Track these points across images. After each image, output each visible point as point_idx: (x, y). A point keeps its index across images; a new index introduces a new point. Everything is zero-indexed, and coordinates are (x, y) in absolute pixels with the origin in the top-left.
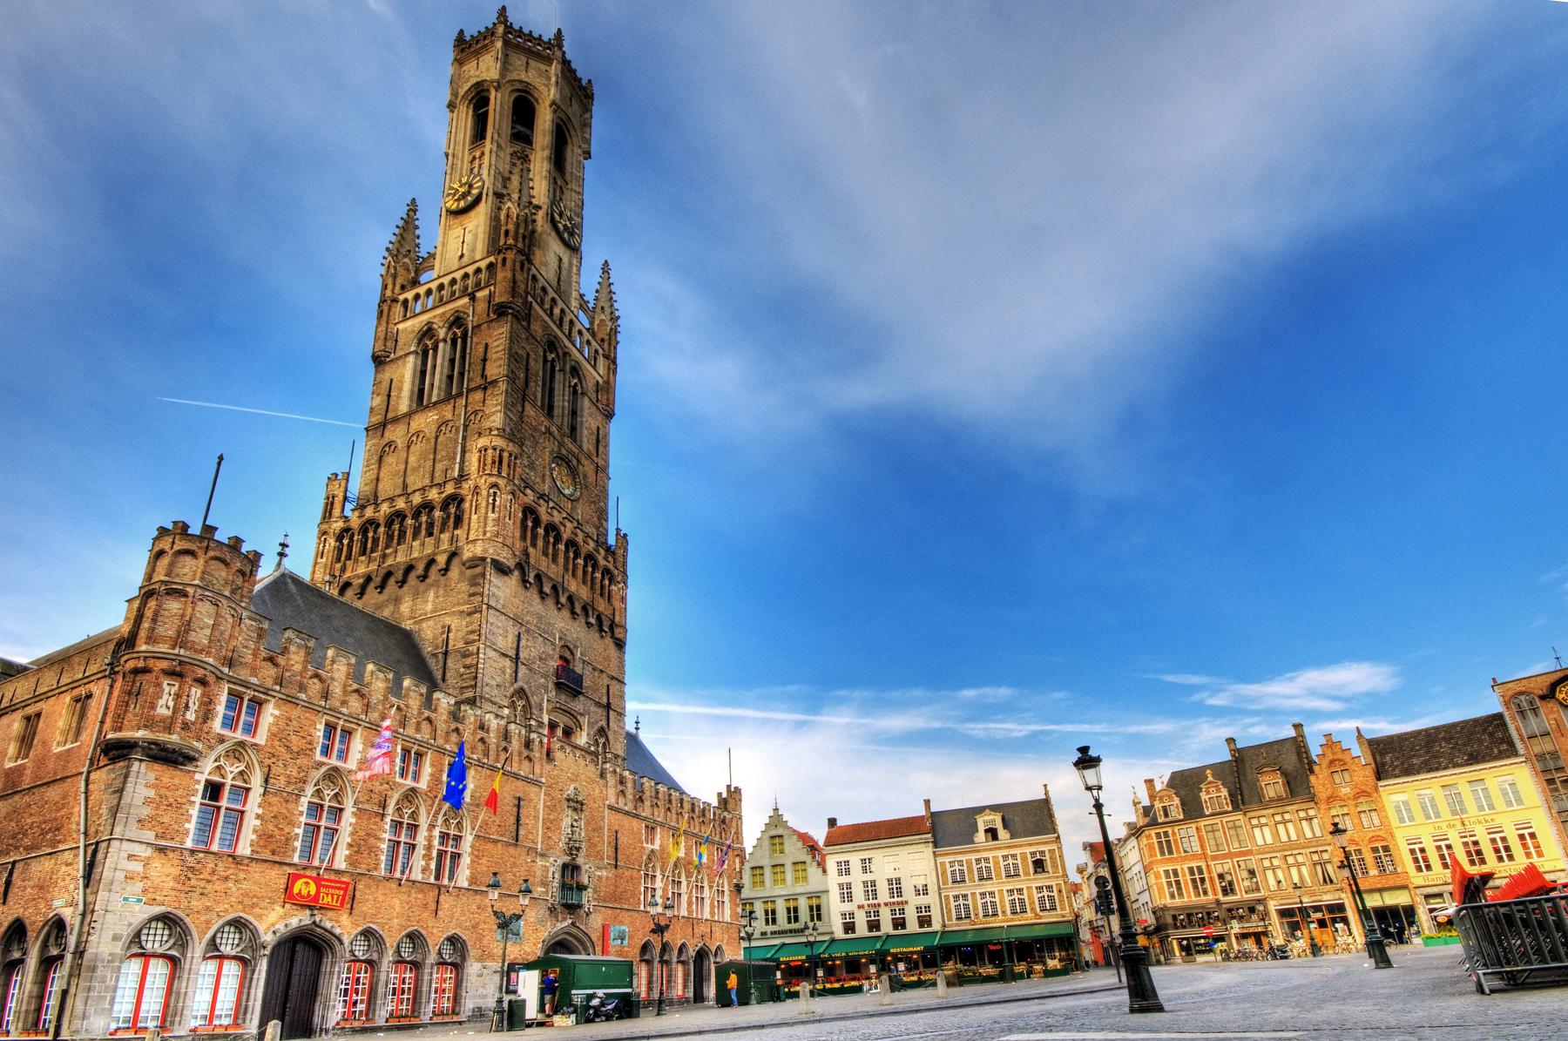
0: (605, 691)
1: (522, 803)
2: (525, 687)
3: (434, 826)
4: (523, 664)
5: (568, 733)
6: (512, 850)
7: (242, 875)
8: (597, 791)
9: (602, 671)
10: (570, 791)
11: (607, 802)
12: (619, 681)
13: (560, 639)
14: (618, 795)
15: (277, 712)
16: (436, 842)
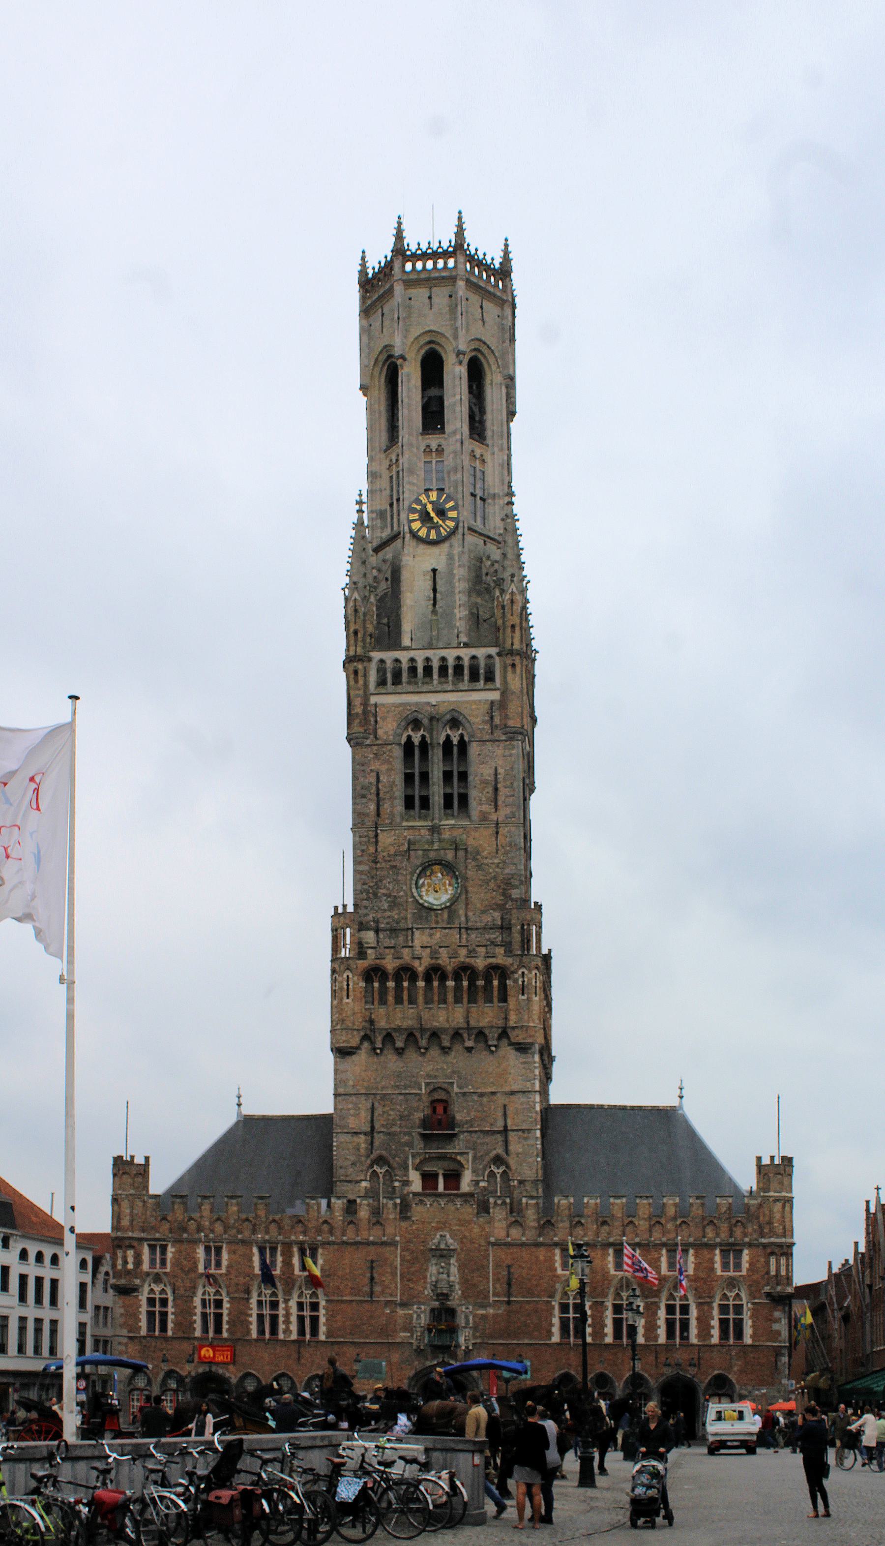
0: (500, 1114)
1: (374, 1264)
2: (384, 1153)
3: (289, 1300)
4: (379, 1132)
5: (454, 1178)
6: (367, 1306)
7: (169, 1347)
8: (476, 1230)
9: (493, 1093)
10: (432, 1244)
11: (492, 1239)
12: (524, 1092)
13: (427, 1084)
14: (510, 1226)
15: (173, 1250)
16: (294, 1310)
